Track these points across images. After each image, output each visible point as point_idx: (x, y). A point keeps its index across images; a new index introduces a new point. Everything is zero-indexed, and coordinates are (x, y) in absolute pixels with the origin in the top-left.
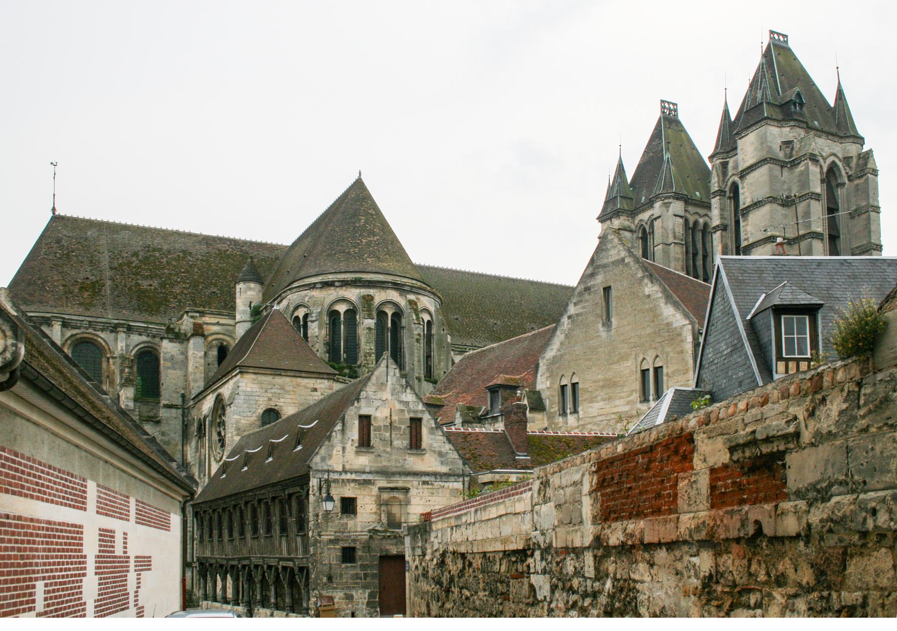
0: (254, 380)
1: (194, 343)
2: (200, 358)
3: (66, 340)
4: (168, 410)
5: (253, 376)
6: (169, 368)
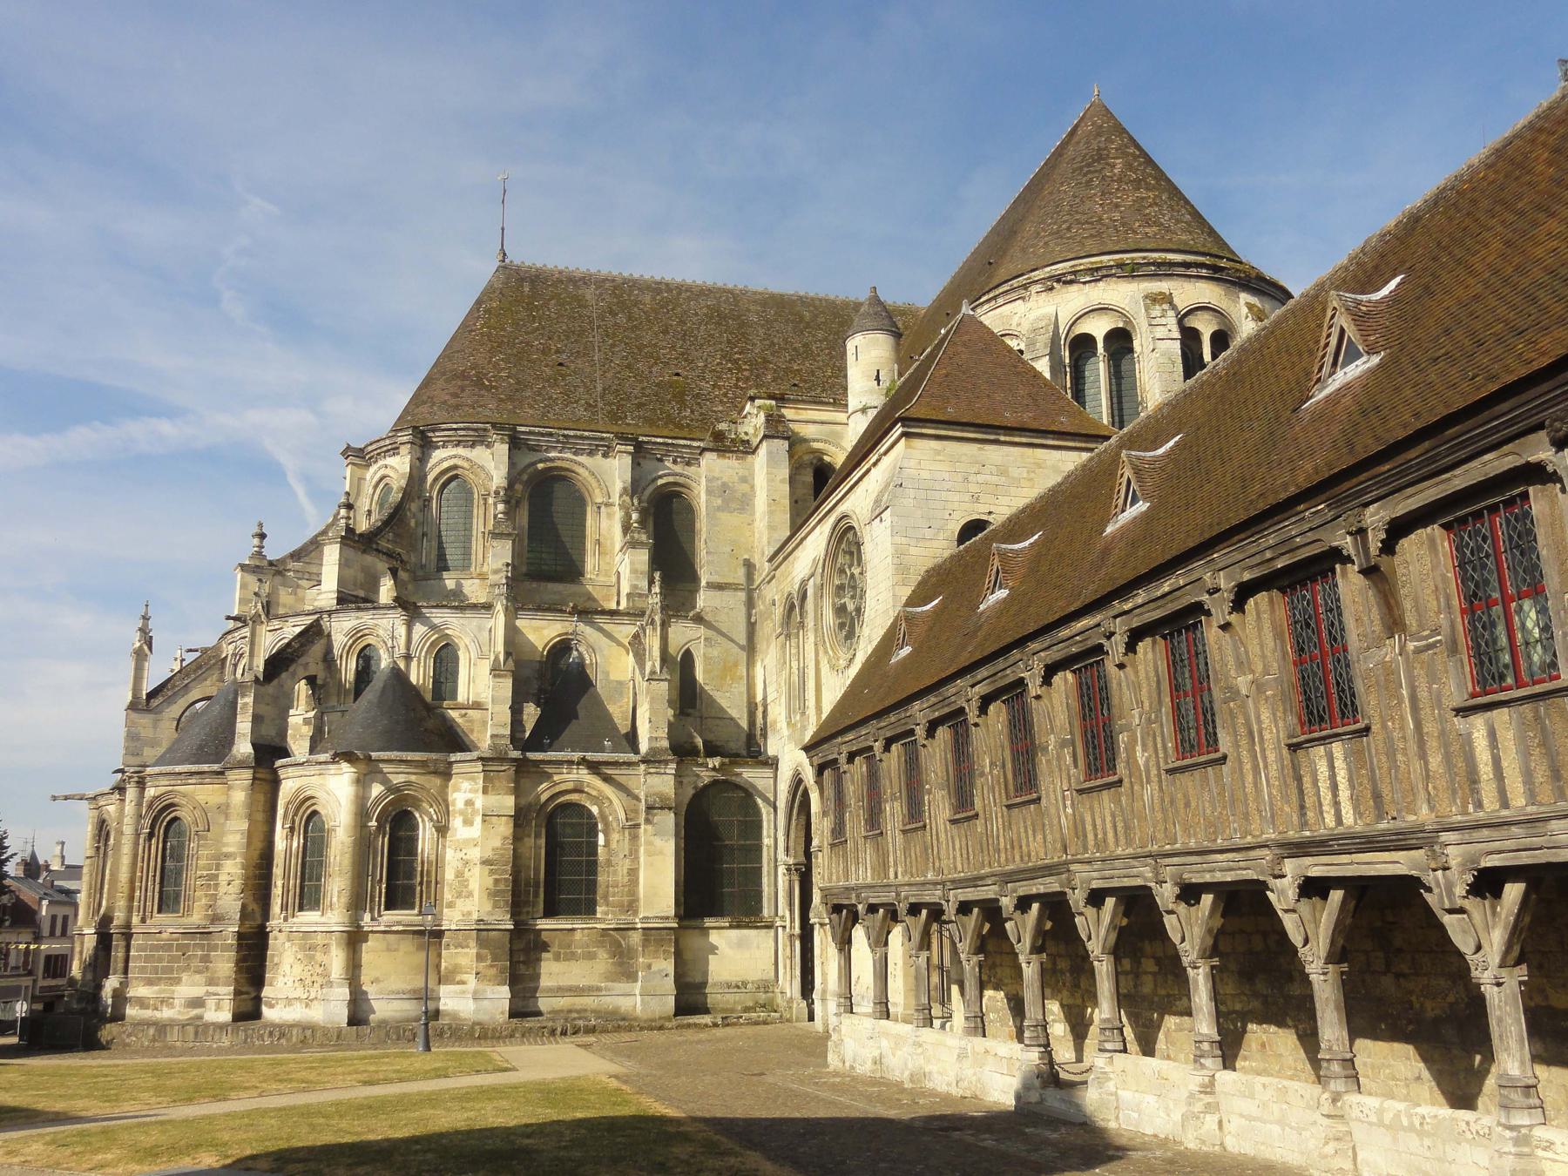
0: (938, 452)
1: (769, 453)
2: (782, 481)
3: (520, 474)
5: (934, 444)
6: (719, 509)
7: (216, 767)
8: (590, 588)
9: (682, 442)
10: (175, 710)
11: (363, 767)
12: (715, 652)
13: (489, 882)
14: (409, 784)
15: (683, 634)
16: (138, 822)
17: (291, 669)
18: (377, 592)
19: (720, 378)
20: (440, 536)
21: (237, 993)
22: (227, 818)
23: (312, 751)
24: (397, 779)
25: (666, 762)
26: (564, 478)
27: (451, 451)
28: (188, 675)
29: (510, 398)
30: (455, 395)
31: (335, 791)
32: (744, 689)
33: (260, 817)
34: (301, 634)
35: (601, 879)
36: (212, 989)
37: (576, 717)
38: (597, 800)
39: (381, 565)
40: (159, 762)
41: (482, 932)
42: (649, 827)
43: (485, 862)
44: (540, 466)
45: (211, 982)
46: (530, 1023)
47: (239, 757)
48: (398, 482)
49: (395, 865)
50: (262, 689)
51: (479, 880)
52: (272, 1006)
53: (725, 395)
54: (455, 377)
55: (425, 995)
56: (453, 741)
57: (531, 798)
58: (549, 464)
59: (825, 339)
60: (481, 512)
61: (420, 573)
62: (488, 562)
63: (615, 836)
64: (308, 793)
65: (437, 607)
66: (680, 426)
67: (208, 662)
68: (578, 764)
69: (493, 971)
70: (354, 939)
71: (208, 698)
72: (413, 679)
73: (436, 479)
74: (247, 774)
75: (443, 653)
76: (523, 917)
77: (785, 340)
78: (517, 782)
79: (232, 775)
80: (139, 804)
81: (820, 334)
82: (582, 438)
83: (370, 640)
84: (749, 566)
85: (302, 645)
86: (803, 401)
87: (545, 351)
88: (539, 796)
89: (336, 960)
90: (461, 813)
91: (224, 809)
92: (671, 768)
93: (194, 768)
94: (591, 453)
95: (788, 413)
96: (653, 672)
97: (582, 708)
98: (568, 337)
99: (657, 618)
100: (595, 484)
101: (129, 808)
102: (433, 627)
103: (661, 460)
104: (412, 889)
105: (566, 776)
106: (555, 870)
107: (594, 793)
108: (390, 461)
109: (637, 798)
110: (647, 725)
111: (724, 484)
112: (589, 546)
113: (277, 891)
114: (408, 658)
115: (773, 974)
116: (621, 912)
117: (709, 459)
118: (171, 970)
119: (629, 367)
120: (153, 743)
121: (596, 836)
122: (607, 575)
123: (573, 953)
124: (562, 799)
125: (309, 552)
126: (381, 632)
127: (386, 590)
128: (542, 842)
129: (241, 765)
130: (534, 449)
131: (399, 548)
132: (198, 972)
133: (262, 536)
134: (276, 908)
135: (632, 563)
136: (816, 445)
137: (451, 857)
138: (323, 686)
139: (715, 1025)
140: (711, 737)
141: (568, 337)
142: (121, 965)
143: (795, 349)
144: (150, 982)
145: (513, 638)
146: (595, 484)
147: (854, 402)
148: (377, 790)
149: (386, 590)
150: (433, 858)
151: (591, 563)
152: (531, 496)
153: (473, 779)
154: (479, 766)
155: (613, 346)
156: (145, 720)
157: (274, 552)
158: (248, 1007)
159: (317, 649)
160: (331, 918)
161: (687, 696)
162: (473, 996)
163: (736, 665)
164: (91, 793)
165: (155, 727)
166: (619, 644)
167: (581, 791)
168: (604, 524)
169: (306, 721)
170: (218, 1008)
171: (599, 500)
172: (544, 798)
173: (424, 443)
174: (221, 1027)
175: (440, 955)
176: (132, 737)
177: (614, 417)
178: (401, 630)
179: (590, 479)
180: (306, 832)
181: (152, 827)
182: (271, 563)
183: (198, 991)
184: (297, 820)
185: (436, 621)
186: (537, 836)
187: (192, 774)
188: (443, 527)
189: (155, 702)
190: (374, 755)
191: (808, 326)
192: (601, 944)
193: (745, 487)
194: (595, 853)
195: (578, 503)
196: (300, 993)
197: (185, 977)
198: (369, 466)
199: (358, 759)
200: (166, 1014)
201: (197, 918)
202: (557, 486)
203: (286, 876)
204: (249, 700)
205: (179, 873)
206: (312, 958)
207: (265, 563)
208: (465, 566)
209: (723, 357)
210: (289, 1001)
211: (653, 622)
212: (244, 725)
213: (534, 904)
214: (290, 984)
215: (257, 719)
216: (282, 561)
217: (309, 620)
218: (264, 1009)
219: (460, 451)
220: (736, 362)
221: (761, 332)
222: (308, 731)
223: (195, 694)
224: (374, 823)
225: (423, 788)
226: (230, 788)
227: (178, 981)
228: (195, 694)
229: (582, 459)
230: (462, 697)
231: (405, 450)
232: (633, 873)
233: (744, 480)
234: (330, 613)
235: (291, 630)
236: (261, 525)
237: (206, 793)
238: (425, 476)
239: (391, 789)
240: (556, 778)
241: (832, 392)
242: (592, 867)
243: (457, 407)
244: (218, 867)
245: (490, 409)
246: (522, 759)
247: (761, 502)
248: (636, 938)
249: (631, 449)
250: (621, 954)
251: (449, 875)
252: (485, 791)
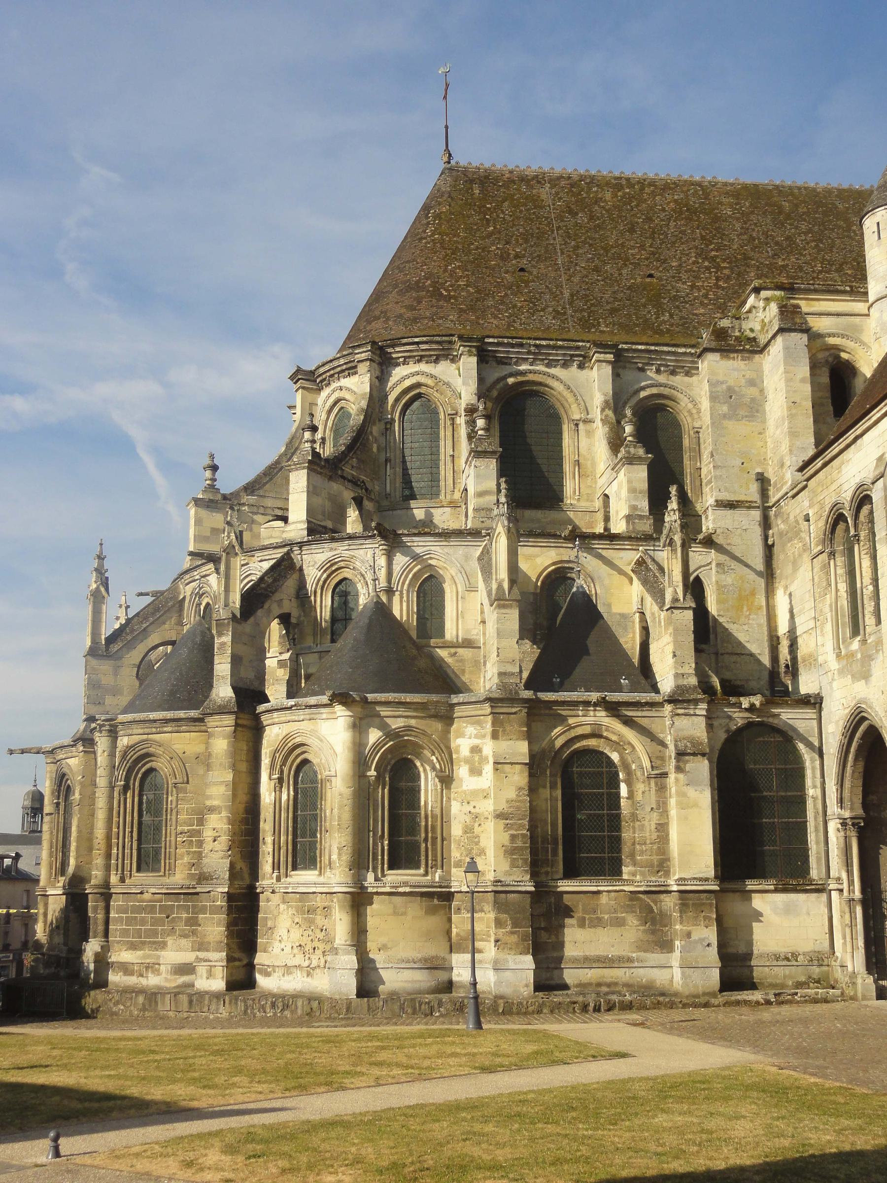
1: (786, 348)
2: (803, 380)
4: (729, 513)
6: (725, 416)
7: (193, 713)
8: (571, 515)
9: (665, 349)
10: (135, 656)
11: (358, 709)
12: (729, 579)
13: (505, 838)
14: (408, 728)
16: (111, 774)
17: (266, 606)
18: (344, 523)
19: (697, 278)
20: (404, 462)
21: (230, 959)
22: (208, 767)
23: (290, 696)
24: (396, 724)
25: (696, 702)
26: (536, 394)
27: (412, 368)
28: (146, 619)
29: (472, 308)
30: (411, 308)
31: (330, 737)
32: (763, 620)
33: (243, 767)
34: (273, 568)
35: (626, 835)
36: (202, 955)
37: (588, 654)
38: (617, 746)
39: (348, 495)
40: (124, 712)
41: (500, 895)
42: (681, 776)
43: (500, 816)
44: (511, 380)
45: (201, 946)
46: (558, 997)
47: (219, 702)
48: (356, 407)
49: (396, 822)
50: (239, 627)
52: (267, 974)
53: (706, 296)
54: (409, 288)
55: (435, 965)
57: (544, 744)
58: (520, 379)
59: (810, 231)
60: (449, 433)
61: (385, 503)
62: (471, 480)
63: (640, 787)
64: (298, 740)
65: (415, 535)
66: (661, 333)
67: (165, 605)
68: (596, 705)
69: (514, 939)
70: (359, 901)
71: (173, 643)
72: (396, 612)
73: (397, 400)
74: (229, 720)
75: (427, 587)
76: (543, 878)
77: (766, 234)
78: (528, 725)
79: (212, 722)
80: (112, 755)
81: (804, 227)
82: (555, 347)
83: (346, 573)
84: (763, 481)
85: (275, 580)
86: (816, 291)
87: (504, 257)
88: (552, 742)
89: (340, 925)
90: (467, 761)
91: (205, 760)
92: (702, 709)
93: (169, 715)
94: (566, 365)
96: (675, 600)
97: (591, 642)
98: (526, 241)
99: (677, 538)
100: (571, 399)
101: (102, 759)
102: (416, 557)
103: (642, 370)
104: (415, 847)
105: (586, 721)
106: (576, 823)
107: (614, 738)
108: (345, 382)
109: (663, 744)
110: (670, 660)
111: (730, 389)
112: (567, 467)
113: (267, 848)
114: (390, 591)
115: (826, 944)
116: (651, 873)
117: (710, 364)
118: (155, 933)
119: (597, 270)
120: (115, 691)
121: (618, 787)
122: (590, 499)
123: (599, 919)
124: (577, 745)
126: (358, 564)
127: (353, 521)
128: (559, 793)
129: (221, 710)
130: (503, 362)
131: (370, 475)
132: (185, 936)
133: (214, 468)
134: (266, 865)
135: (629, 481)
136: (832, 341)
137: (456, 808)
138: (297, 624)
139: (768, 1002)
140: (728, 675)
141: (526, 241)
142: (101, 928)
143: (777, 243)
144: (133, 947)
146: (571, 399)
148: (374, 735)
149: (353, 521)
150: (438, 811)
151: (570, 487)
152: (501, 416)
153: (479, 723)
154: (487, 708)
155: (577, 247)
156: (105, 667)
157: (229, 483)
158: (240, 975)
159: (290, 584)
160: (332, 876)
162: (498, 967)
163: (753, 593)
164: (48, 746)
165: (116, 674)
166: (621, 572)
167: (600, 736)
168: (584, 442)
169: (281, 664)
170: (210, 975)
171: (576, 416)
172: (559, 743)
173: (383, 362)
174: (217, 996)
175: (450, 920)
176: (93, 685)
177: (586, 325)
178: (382, 561)
179: (566, 393)
180: (296, 783)
181: (127, 779)
182: (225, 497)
183: (188, 957)
184: (286, 770)
185: (418, 550)
186: (553, 787)
187: (167, 721)
188: (407, 452)
189: (115, 648)
190: (370, 697)
191: (788, 217)
192: (630, 909)
193: (753, 392)
194: (618, 807)
195: (553, 420)
196: (299, 960)
197: (170, 941)
198: (320, 390)
199: (354, 701)
200: (152, 981)
201: (179, 877)
202: (529, 402)
203: (276, 832)
204: (227, 639)
205: (158, 829)
206: (311, 922)
207: (219, 497)
208: (433, 491)
209: (698, 255)
210: (288, 969)
211: (671, 543)
212: (222, 667)
213: (553, 864)
214: (288, 949)
215: (236, 660)
216: (236, 495)
217: (278, 554)
218: (259, 977)
219: (423, 367)
220: (713, 259)
221: (738, 226)
222: (283, 674)
223: (154, 639)
224: (372, 773)
225: (424, 733)
226: (210, 735)
227: (163, 946)
228: (154, 639)
229: (556, 371)
230: (450, 632)
231: (363, 368)
232: (662, 828)
233: (752, 383)
234: (301, 545)
235: (259, 566)
236: (212, 456)
237: (184, 742)
238: (386, 397)
239: (390, 735)
240: (571, 721)
242: (615, 822)
243: (415, 320)
244: (201, 822)
245: (451, 321)
246: (531, 703)
248: (669, 903)
249: (610, 357)
250: (654, 921)
251: (456, 830)
252: (495, 736)
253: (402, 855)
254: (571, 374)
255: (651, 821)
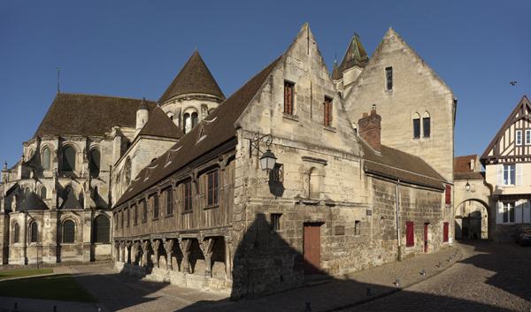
15: (95, 182)
31: (20, 218)
41: (50, 247)
49: (34, 235)
51: (50, 236)
56: (45, 207)
70: (25, 248)
89: (22, 253)
95: (122, 130)
105: (68, 215)
106: (65, 233)
113: (10, 239)
125: (15, 167)
127: (32, 174)
137: (44, 232)
145: (57, 185)
147: (137, 127)
149: (32, 174)
157: (9, 168)
160: (20, 244)
161: (95, 194)
162: (50, 259)
235: (12, 185)
241: (132, 124)
247: (114, 152)
253: (33, 240)
254: (78, 142)
255: (80, 232)
